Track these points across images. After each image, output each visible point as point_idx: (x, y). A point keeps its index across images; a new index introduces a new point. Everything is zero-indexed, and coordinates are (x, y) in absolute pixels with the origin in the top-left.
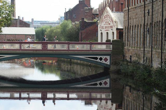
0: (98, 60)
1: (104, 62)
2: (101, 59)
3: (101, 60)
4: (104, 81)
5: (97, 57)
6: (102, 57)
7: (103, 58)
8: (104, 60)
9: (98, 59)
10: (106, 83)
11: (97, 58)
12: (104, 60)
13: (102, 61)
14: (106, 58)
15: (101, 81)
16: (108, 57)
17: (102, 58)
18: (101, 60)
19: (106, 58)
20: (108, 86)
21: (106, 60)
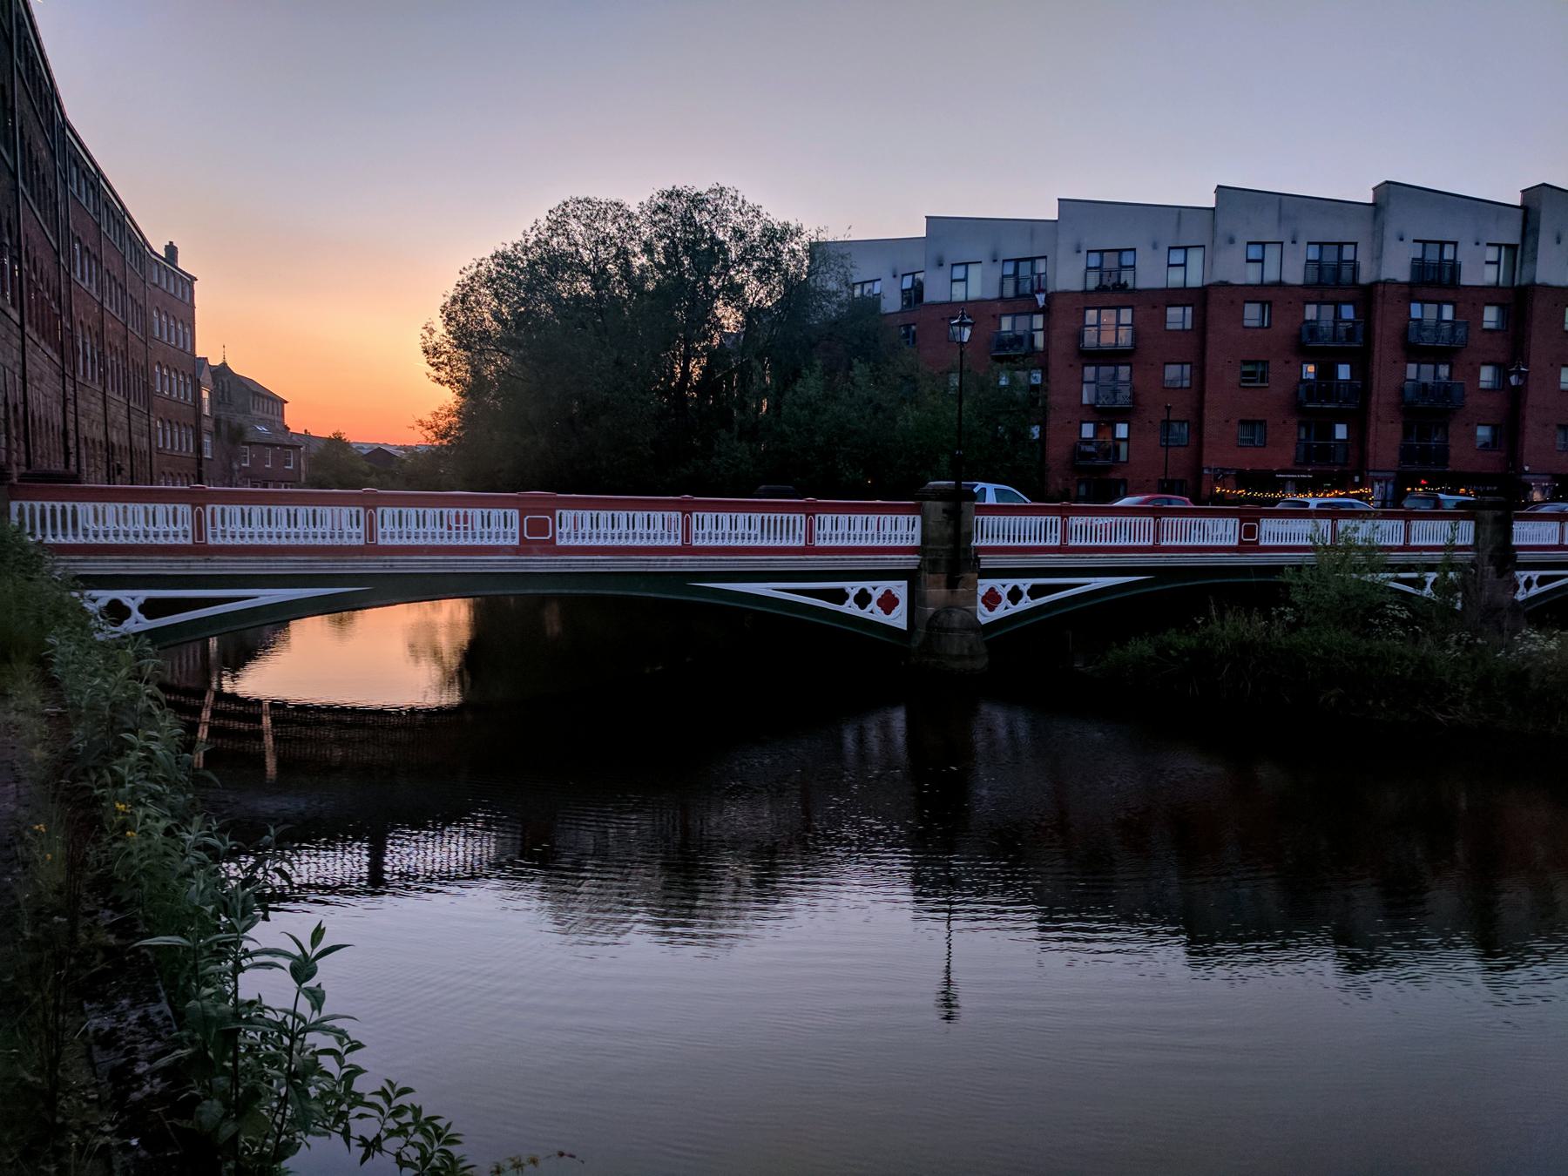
0: (850, 608)
2: (863, 599)
3: (862, 607)
5: (842, 590)
6: (867, 585)
7: (876, 595)
8: (879, 603)
9: (850, 601)
12: (879, 603)
13: (869, 608)
14: (888, 592)
16: (900, 588)
17: (870, 591)
18: (862, 607)
19: (888, 592)
21: (888, 602)
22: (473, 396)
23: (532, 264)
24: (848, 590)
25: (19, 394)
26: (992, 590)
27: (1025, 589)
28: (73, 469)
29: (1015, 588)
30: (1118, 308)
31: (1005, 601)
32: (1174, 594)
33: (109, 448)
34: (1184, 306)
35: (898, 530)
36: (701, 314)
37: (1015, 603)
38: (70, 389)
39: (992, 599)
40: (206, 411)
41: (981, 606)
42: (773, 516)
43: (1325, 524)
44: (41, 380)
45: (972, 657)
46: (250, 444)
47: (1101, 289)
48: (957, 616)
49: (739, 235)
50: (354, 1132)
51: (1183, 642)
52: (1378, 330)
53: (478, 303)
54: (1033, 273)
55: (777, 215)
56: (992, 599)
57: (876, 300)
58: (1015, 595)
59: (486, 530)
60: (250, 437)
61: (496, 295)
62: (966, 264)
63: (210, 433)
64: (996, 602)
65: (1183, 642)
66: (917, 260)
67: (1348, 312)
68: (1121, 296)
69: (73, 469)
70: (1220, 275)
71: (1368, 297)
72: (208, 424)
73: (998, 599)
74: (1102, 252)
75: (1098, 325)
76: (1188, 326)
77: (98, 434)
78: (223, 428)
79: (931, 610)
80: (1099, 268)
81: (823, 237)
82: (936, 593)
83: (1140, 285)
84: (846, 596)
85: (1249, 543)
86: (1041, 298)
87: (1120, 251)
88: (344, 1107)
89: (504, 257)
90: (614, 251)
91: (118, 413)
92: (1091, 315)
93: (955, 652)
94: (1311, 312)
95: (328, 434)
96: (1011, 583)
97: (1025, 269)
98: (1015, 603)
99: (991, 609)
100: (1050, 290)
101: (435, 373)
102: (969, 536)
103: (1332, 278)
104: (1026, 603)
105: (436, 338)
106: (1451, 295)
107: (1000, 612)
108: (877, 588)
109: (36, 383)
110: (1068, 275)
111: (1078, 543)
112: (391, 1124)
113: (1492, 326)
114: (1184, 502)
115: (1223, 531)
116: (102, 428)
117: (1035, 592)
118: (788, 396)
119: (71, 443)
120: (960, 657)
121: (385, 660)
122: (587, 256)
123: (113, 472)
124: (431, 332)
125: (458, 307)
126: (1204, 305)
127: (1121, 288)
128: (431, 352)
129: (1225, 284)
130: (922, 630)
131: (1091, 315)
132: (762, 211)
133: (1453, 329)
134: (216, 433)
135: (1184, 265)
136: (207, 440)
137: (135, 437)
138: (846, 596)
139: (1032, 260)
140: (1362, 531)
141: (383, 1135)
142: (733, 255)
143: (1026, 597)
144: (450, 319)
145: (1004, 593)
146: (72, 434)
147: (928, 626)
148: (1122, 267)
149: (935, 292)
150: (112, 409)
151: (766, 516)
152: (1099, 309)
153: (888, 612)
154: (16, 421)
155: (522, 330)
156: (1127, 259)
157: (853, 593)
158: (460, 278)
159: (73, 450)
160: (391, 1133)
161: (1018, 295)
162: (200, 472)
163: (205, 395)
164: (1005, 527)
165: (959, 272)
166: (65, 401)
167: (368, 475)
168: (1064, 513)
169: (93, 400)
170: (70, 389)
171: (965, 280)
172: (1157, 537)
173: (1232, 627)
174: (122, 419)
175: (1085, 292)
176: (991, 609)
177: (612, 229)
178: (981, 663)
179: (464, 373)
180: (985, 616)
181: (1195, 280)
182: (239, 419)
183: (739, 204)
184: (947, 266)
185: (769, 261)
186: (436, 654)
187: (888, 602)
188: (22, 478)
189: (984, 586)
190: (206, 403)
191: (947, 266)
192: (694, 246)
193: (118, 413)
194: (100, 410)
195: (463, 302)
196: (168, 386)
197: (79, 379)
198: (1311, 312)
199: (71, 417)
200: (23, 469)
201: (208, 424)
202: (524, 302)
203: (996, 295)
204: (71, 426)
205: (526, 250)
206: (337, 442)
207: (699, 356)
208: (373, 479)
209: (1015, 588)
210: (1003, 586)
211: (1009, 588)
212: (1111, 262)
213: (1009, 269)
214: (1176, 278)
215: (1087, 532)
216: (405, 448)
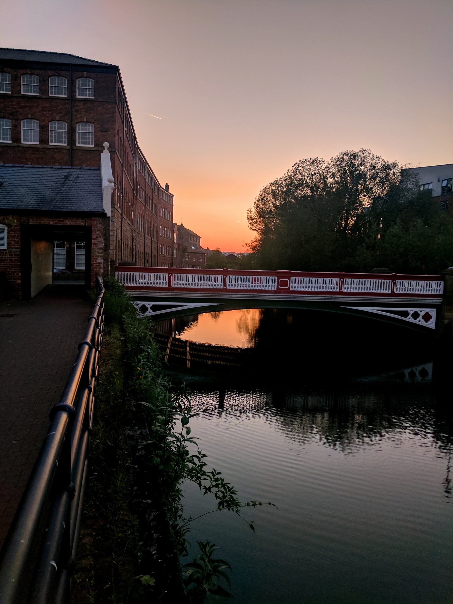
0: (409, 319)
2: (416, 315)
3: (415, 319)
4: (420, 368)
6: (418, 310)
7: (422, 314)
8: (423, 317)
9: (410, 316)
10: (424, 373)
12: (423, 317)
13: (418, 319)
14: (427, 313)
16: (433, 312)
17: (419, 312)
18: (415, 319)
19: (427, 313)
21: (427, 317)
22: (265, 235)
24: (409, 312)
25: (120, 237)
28: (134, 261)
33: (145, 254)
38: (134, 235)
40: (175, 242)
44: (126, 232)
46: (189, 253)
50: (203, 484)
59: (268, 284)
60: (189, 250)
63: (176, 249)
69: (134, 261)
72: (176, 246)
77: (142, 249)
78: (181, 247)
84: (408, 314)
88: (199, 475)
91: (148, 242)
95: (214, 249)
101: (251, 227)
105: (253, 214)
108: (422, 311)
109: (125, 233)
112: (214, 483)
116: (143, 248)
118: (388, 232)
119: (134, 253)
123: (146, 262)
128: (250, 219)
134: (178, 249)
136: (175, 251)
137: (153, 250)
138: (408, 314)
141: (211, 486)
146: (134, 250)
150: (147, 241)
153: (427, 321)
154: (119, 246)
155: (283, 209)
157: (411, 313)
159: (134, 255)
160: (214, 486)
162: (172, 262)
163: (175, 236)
166: (133, 238)
169: (141, 238)
170: (134, 235)
174: (150, 244)
179: (261, 226)
182: (186, 244)
187: (427, 317)
188: (120, 264)
190: (175, 238)
192: (351, 171)
193: (148, 242)
194: (143, 241)
196: (164, 233)
197: (137, 231)
199: (134, 244)
200: (120, 261)
201: (176, 246)
204: (134, 247)
206: (217, 252)
207: (352, 216)
208: (229, 265)
216: (240, 254)
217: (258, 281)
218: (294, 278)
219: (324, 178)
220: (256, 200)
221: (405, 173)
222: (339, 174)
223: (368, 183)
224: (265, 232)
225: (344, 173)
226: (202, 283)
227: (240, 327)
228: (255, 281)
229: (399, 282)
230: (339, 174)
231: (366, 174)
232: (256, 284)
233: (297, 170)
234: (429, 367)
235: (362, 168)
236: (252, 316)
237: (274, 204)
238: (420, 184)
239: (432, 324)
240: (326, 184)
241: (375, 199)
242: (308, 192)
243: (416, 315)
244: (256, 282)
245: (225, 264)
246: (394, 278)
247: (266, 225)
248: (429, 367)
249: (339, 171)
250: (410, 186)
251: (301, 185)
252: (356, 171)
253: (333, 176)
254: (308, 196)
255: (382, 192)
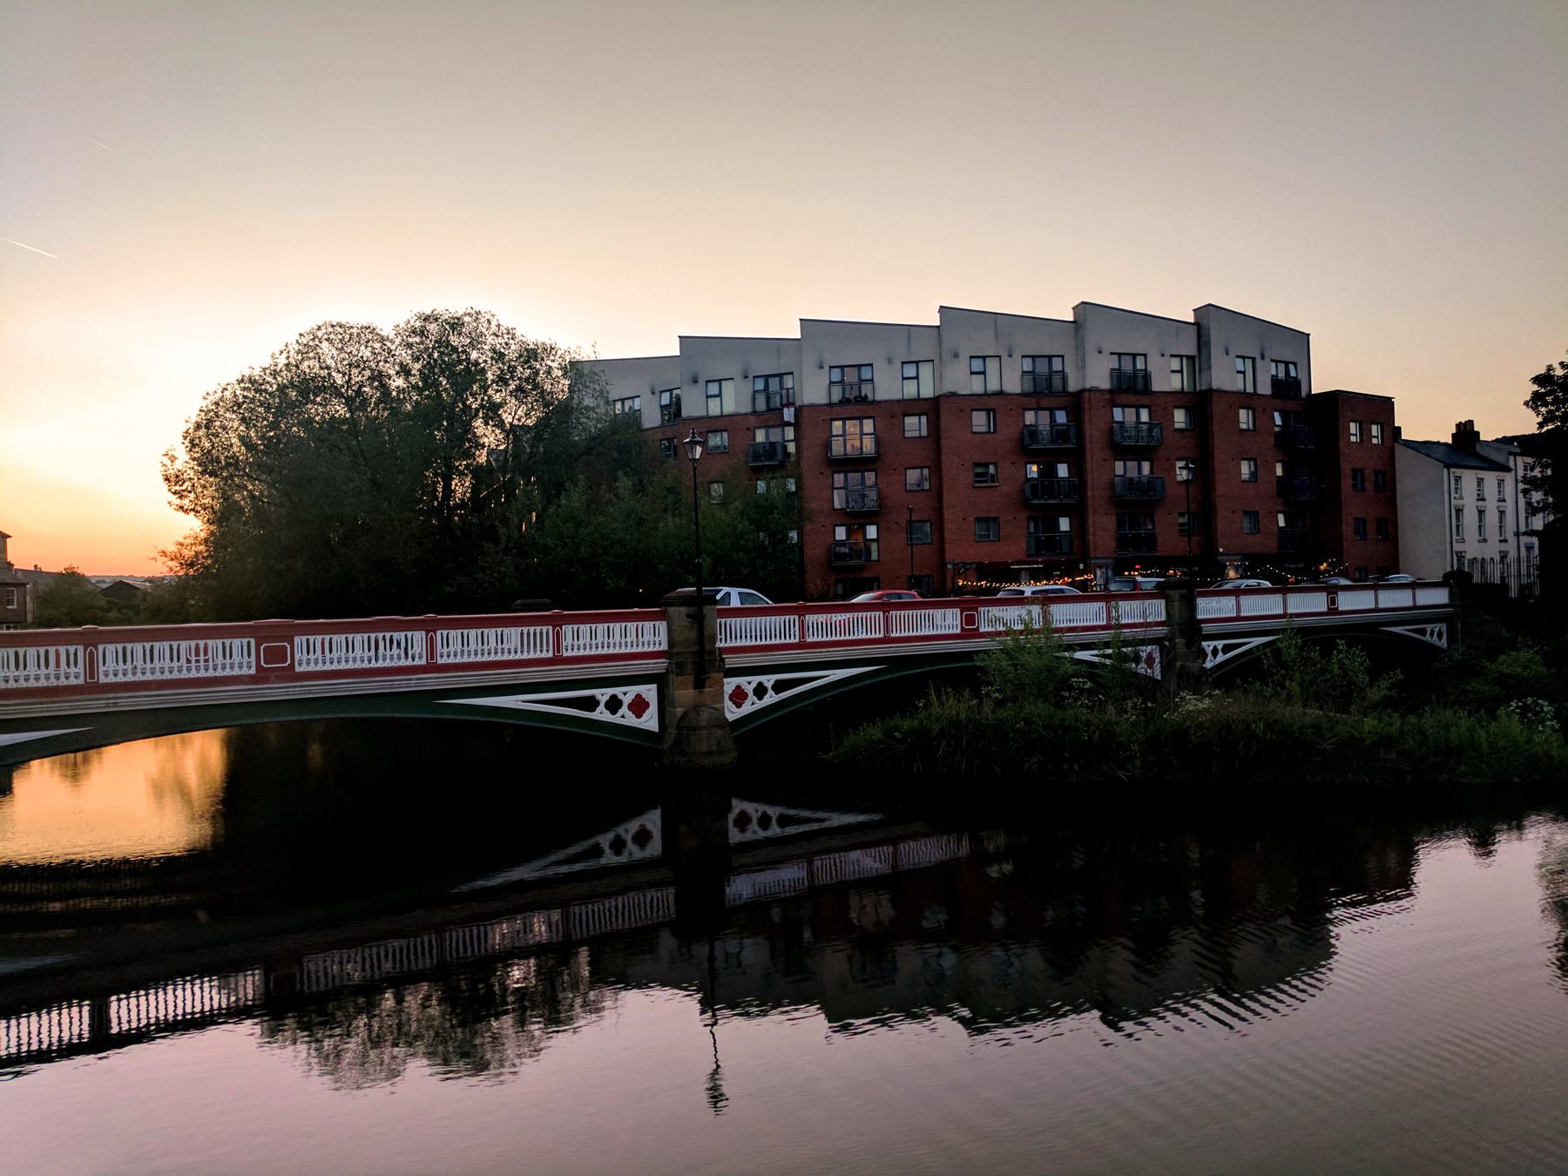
0: (601, 714)
1: (630, 720)
2: (614, 705)
3: (614, 712)
4: (633, 826)
7: (627, 700)
9: (601, 707)
10: (643, 837)
11: (591, 703)
12: (630, 707)
13: (620, 712)
14: (638, 696)
15: (620, 830)
16: (650, 692)
17: (621, 697)
18: (614, 712)
19: (638, 696)
20: (655, 847)
21: (639, 706)
22: (220, 526)
23: (282, 389)
24: (599, 697)
26: (738, 687)
27: (769, 685)
29: (760, 684)
30: (861, 419)
31: (752, 697)
32: (902, 680)
34: (919, 415)
35: (650, 636)
36: (463, 439)
37: (760, 698)
39: (739, 697)
41: (728, 704)
42: (532, 629)
43: (1036, 610)
45: (721, 753)
47: (844, 401)
48: (705, 715)
49: (499, 356)
51: (906, 724)
52: (1088, 432)
53: (224, 428)
54: (781, 387)
55: (533, 334)
56: (739, 697)
57: (634, 418)
58: (760, 691)
61: (243, 420)
62: (720, 381)
64: (742, 699)
65: (906, 724)
66: (674, 377)
67: (1061, 417)
68: (864, 407)
70: (948, 387)
71: (1076, 402)
73: (745, 696)
74: (842, 367)
75: (844, 435)
76: (924, 433)
79: (680, 710)
80: (842, 382)
81: (578, 358)
82: (684, 694)
83: (878, 398)
84: (598, 703)
85: (969, 633)
86: (789, 414)
87: (859, 366)
89: (252, 381)
90: (367, 373)
92: (837, 426)
93: (704, 748)
94: (1030, 418)
96: (756, 679)
97: (774, 385)
98: (760, 698)
99: (739, 706)
100: (798, 403)
101: (178, 502)
102: (713, 639)
103: (1045, 388)
104: (771, 698)
105: (179, 465)
106: (1145, 400)
107: (748, 708)
108: (627, 694)
110: (814, 390)
111: (815, 639)
113: (1182, 426)
114: (913, 595)
115: (947, 620)
117: (779, 687)
120: (710, 754)
121: (132, 803)
122: (339, 379)
124: (173, 459)
125: (202, 432)
126: (938, 417)
127: (862, 400)
128: (173, 479)
129: (953, 394)
130: (672, 731)
131: (837, 426)
132: (518, 333)
133: (1150, 430)
135: (917, 378)
139: (780, 376)
140: (1064, 615)
142: (490, 375)
143: (771, 692)
144: (194, 446)
145: (749, 689)
147: (676, 726)
148: (861, 381)
149: (690, 409)
151: (525, 630)
152: (844, 420)
153: (639, 716)
155: (271, 456)
156: (866, 374)
157: (603, 700)
158: (204, 404)
161: (769, 409)
164: (748, 626)
165: (713, 388)
167: (108, 611)
168: (801, 612)
171: (720, 395)
172: (887, 630)
173: (949, 707)
175: (830, 405)
176: (739, 706)
177: (367, 353)
178: (729, 758)
180: (732, 713)
181: (927, 391)
183: (494, 328)
184: (702, 383)
185: (527, 380)
186: (183, 791)
187: (639, 706)
189: (730, 684)
191: (702, 383)
195: (207, 427)
198: (1030, 418)
202: (274, 426)
203: (749, 410)
205: (275, 374)
206: (71, 579)
208: (113, 614)
209: (760, 684)
210: (748, 683)
211: (754, 685)
212: (851, 376)
213: (760, 385)
214: (910, 390)
215: (828, 628)
216: (150, 580)
217: (206, 654)
218: (304, 638)
219: (379, 377)
220: (191, 426)
221: (576, 370)
222: (417, 366)
223: (490, 392)
224: (223, 517)
225: (430, 366)
226: (22, 673)
227: (158, 790)
228: (197, 654)
229: (568, 629)
230: (417, 366)
231: (483, 371)
232: (193, 664)
233: (308, 349)
234: (653, 820)
235: (474, 355)
236: (201, 756)
237: (241, 438)
238: (612, 397)
239: (650, 721)
240: (384, 388)
241: (513, 432)
242: (340, 410)
243: (614, 705)
244: (202, 658)
245: (100, 614)
246: (557, 622)
247: (225, 498)
248: (653, 820)
249: (416, 359)
250: (588, 402)
251: (323, 389)
252: (460, 362)
253: (405, 371)
254: (344, 421)
255: (527, 415)
